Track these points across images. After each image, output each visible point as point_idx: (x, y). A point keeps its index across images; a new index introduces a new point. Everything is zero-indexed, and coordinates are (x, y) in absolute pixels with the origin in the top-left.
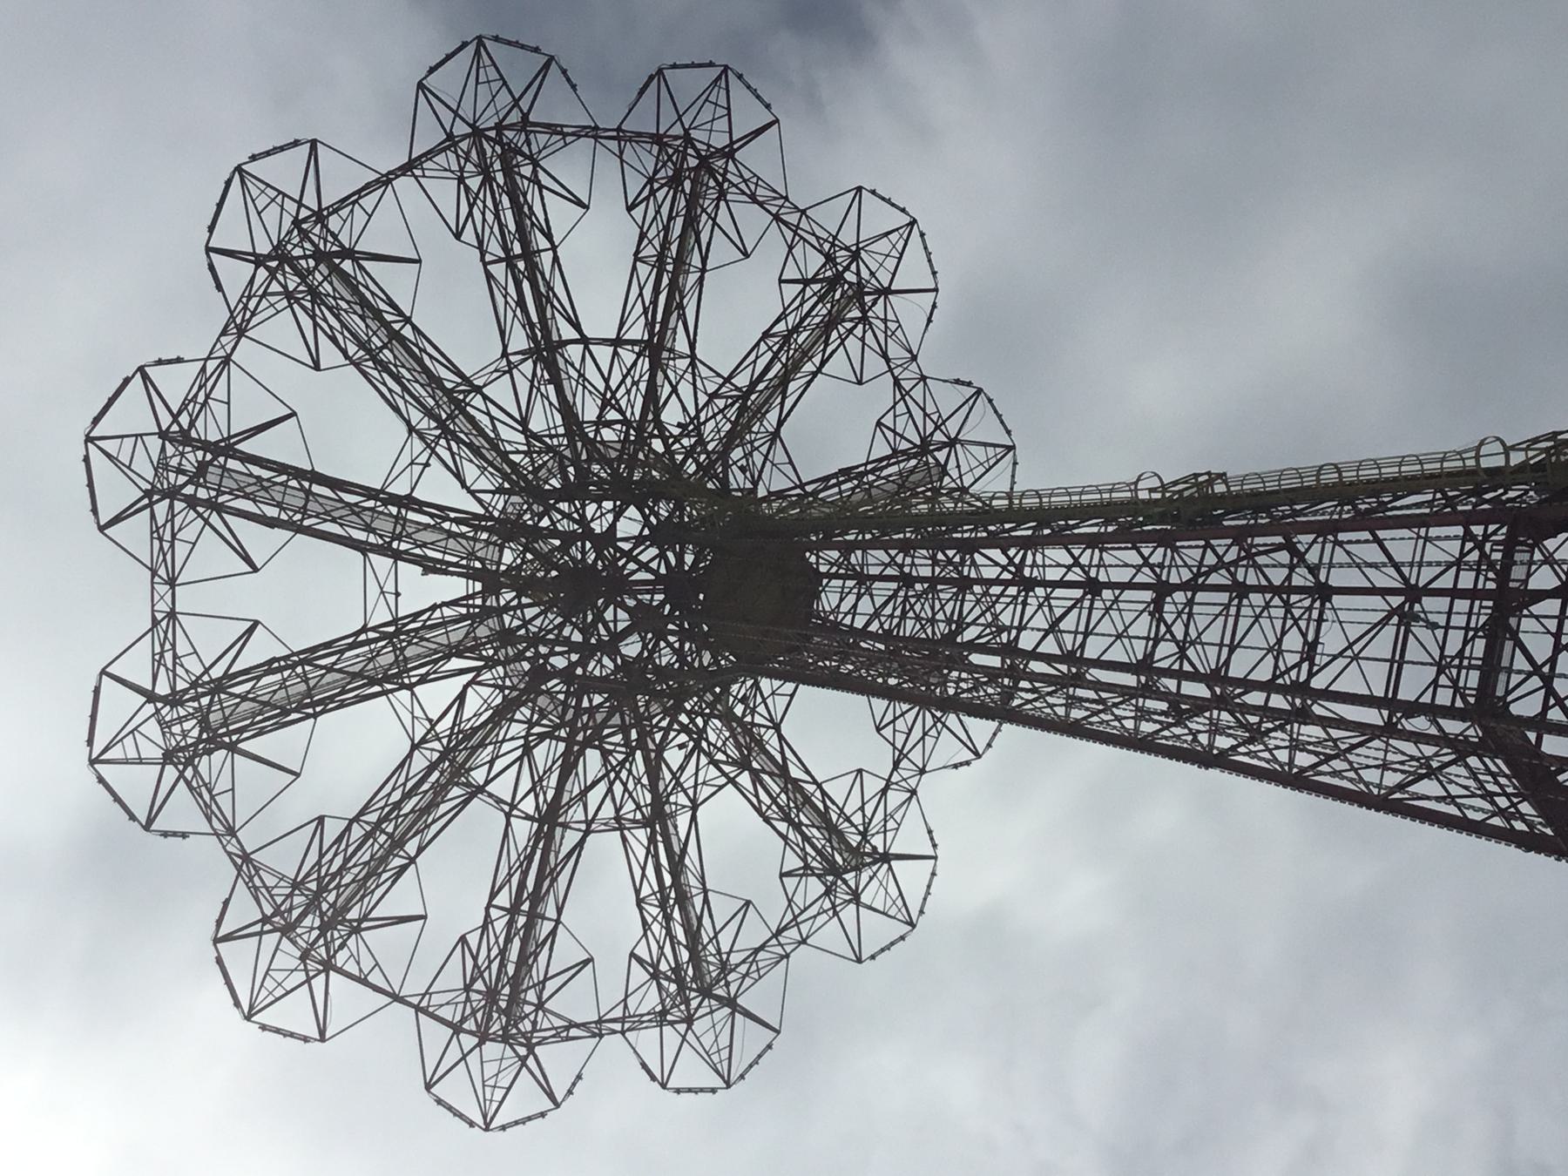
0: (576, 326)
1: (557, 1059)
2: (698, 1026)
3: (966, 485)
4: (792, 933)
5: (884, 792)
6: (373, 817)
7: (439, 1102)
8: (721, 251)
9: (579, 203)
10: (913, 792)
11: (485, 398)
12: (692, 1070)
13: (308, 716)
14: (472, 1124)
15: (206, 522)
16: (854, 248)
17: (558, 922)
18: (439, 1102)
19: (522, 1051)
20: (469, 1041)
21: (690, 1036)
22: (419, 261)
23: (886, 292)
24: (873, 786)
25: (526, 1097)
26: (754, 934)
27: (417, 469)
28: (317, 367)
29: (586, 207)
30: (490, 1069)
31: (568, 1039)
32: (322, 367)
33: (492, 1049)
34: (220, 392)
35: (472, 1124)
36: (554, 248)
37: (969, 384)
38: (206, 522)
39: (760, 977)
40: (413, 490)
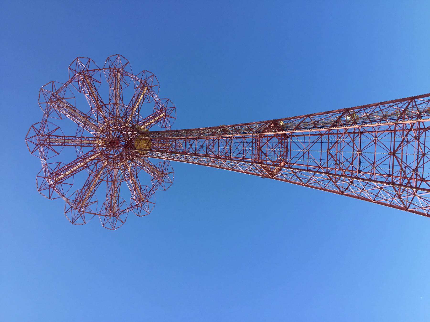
0: (103, 103)
1: (122, 217)
3: (169, 115)
5: (164, 164)
6: (86, 188)
8: (124, 86)
9: (99, 82)
10: (169, 163)
11: (91, 118)
13: (72, 175)
15: (49, 148)
16: (145, 81)
19: (117, 217)
20: (108, 218)
22: (75, 98)
23: (151, 87)
24: (162, 163)
26: (148, 191)
27: (82, 132)
29: (101, 83)
30: (112, 221)
32: (62, 119)
33: (112, 218)
34: (46, 127)
37: (167, 99)
38: (49, 148)
39: (151, 196)
40: (82, 136)
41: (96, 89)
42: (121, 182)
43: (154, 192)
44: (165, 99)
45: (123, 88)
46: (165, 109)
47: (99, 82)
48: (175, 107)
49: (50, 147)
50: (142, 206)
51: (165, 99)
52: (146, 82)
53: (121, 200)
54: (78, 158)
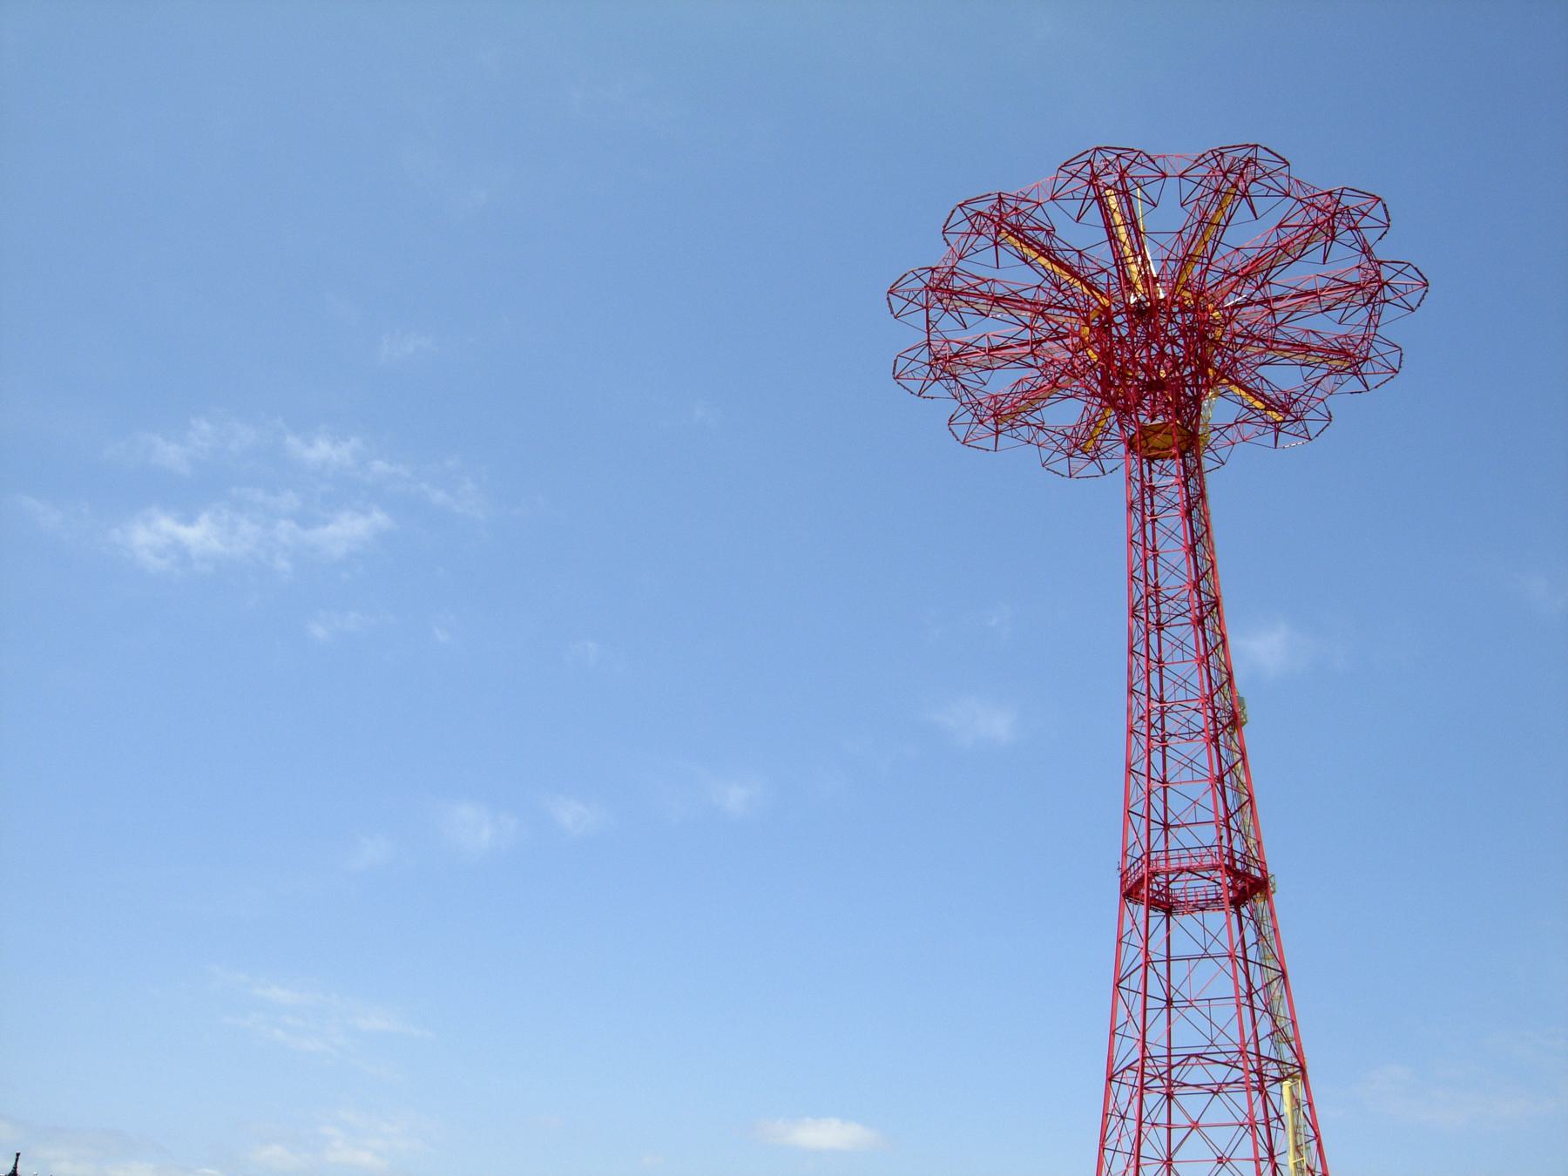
2: (980, 426)
4: (1042, 437)
7: (896, 361)
8: (1335, 314)
9: (1325, 258)
12: (961, 431)
14: (894, 373)
17: (994, 369)
18: (896, 361)
21: (973, 426)
25: (915, 386)
28: (1182, 205)
31: (949, 389)
35: (894, 373)
36: (1295, 260)
38: (1085, 199)
41: (1300, 257)
42: (1037, 368)
43: (1029, 442)
44: (1329, 413)
45: (1325, 313)
46: (1297, 419)
47: (1325, 258)
48: (1310, 439)
49: (1088, 202)
50: (981, 422)
51: (1329, 413)
52: (1365, 359)
53: (985, 375)
54: (1079, 252)
